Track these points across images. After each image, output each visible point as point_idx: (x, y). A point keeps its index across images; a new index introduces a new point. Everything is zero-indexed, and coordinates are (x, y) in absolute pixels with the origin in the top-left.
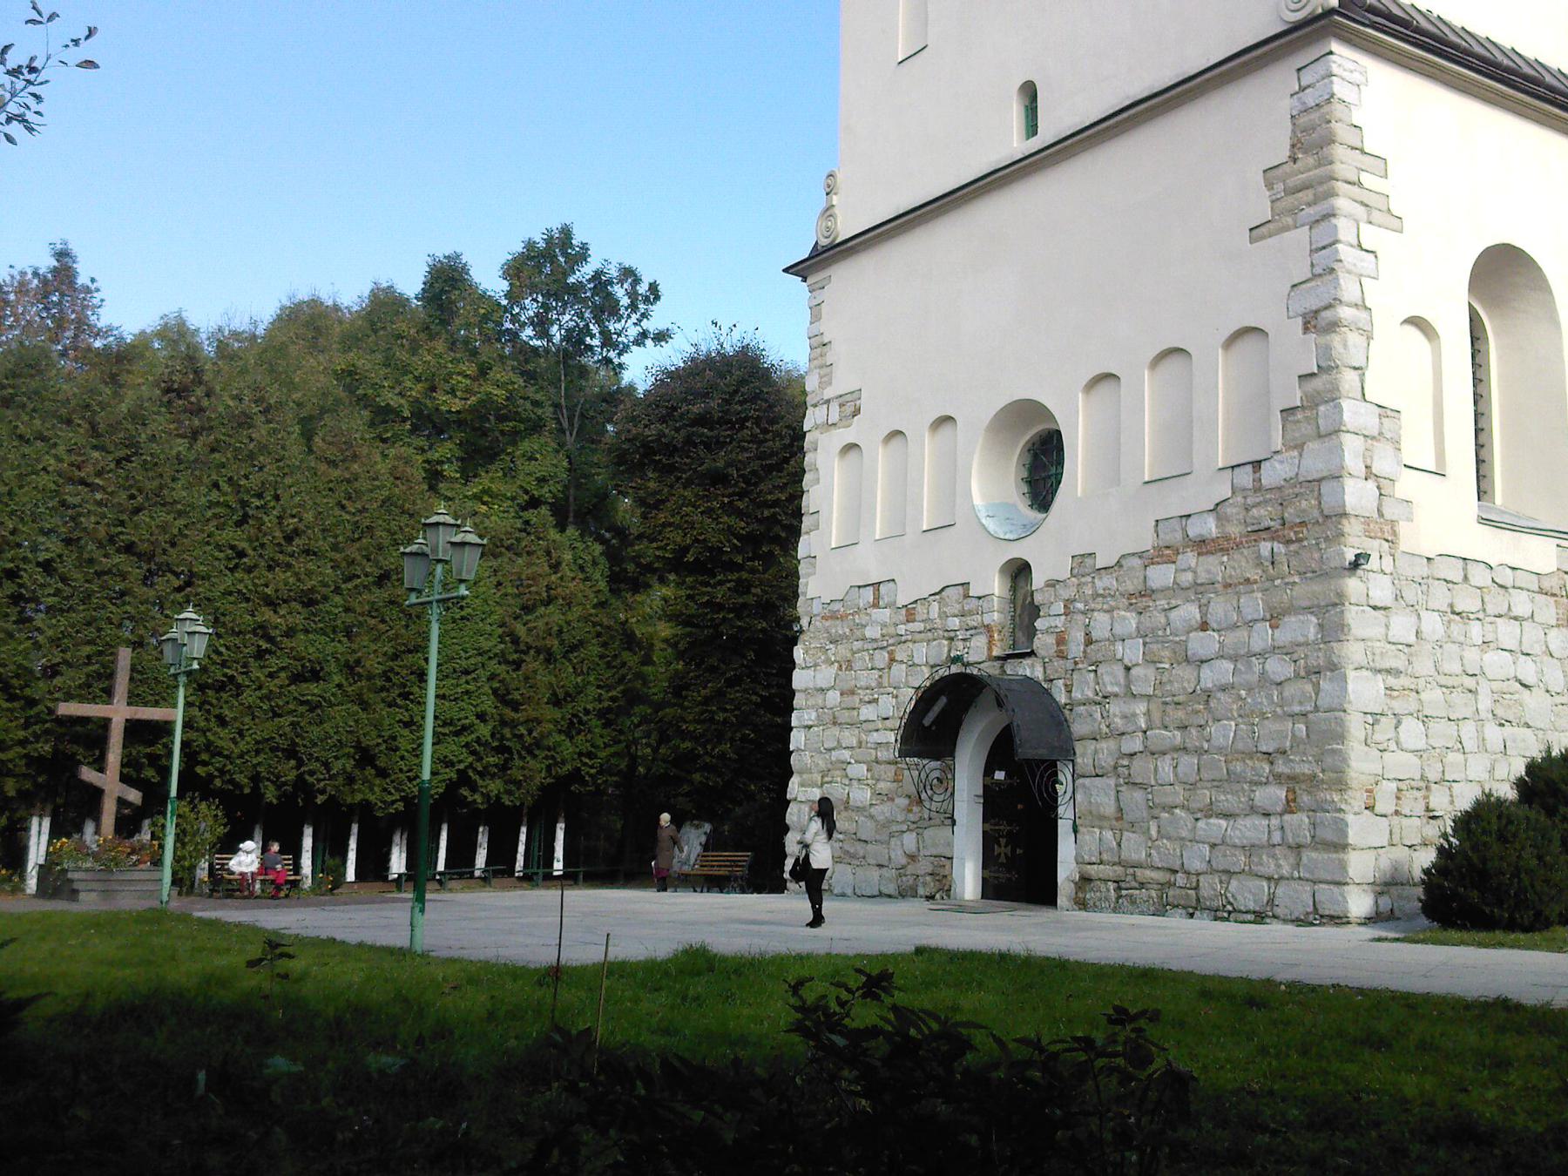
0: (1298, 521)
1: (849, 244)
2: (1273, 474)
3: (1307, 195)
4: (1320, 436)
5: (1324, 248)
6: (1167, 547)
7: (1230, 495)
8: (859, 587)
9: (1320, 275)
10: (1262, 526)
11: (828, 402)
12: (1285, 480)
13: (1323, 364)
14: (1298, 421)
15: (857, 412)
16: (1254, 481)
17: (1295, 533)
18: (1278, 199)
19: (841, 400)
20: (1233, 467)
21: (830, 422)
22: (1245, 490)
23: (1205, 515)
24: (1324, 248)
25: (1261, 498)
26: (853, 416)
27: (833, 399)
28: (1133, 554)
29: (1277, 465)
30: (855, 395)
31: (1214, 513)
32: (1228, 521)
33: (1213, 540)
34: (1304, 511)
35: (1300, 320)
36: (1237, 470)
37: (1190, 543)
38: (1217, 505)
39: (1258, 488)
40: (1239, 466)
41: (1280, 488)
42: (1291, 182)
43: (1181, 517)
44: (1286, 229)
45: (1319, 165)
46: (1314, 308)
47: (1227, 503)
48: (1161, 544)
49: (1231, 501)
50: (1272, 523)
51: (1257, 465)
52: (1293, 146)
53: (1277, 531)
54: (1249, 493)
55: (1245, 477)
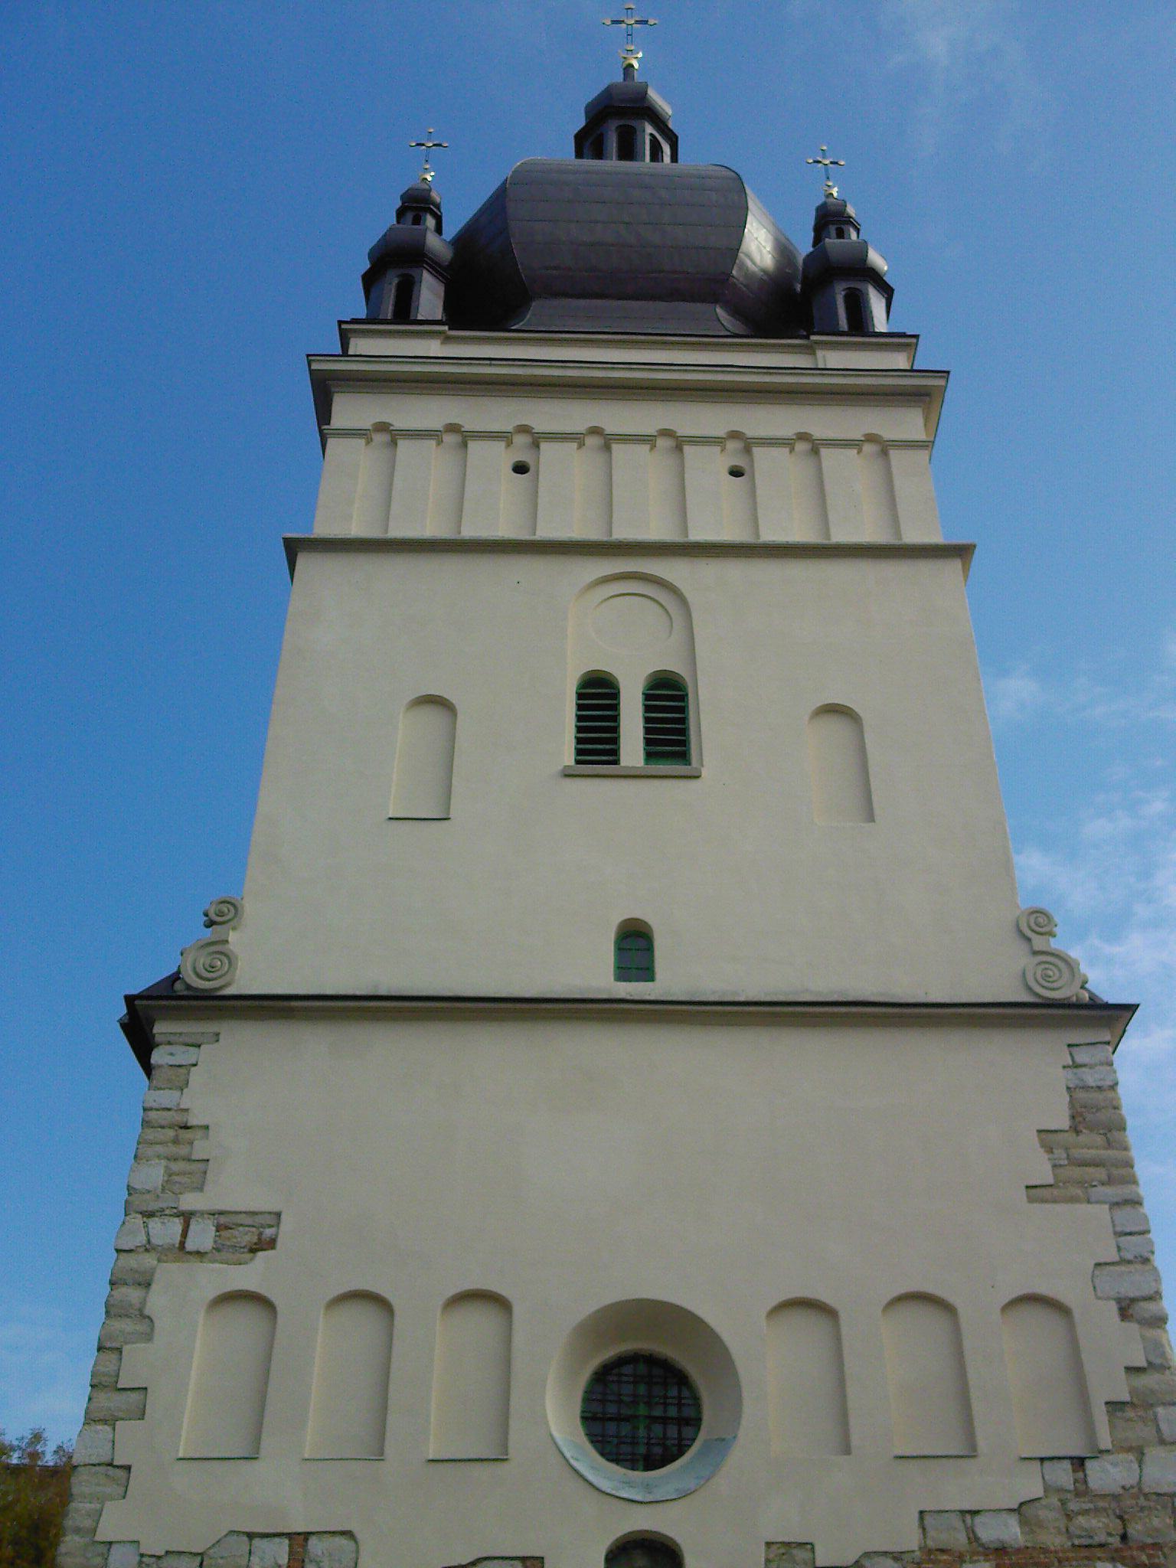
0: (1149, 1541)
1: (294, 1004)
2: (1107, 1475)
3: (1100, 1173)
4: (1162, 1442)
5: (1130, 1234)
6: (942, 1551)
7: (1040, 1493)
8: (251, 1536)
9: (1129, 1262)
10: (1097, 1540)
11: (187, 1217)
12: (1123, 1487)
13: (1152, 1358)
14: (1128, 1420)
15: (271, 1244)
16: (1076, 1481)
17: (1149, 1556)
18: (1061, 1166)
19: (223, 1220)
20: (1042, 1460)
21: (190, 1245)
22: (1061, 1490)
23: (1004, 1515)
24: (1130, 1234)
25: (1091, 1506)
26: (253, 1251)
27: (202, 1213)
28: (885, 1553)
29: (1109, 1467)
30: (269, 1220)
31: (1017, 1512)
32: (1041, 1527)
33: (1018, 1550)
34: (1157, 1530)
35: (1113, 1307)
36: (1047, 1464)
37: (980, 1549)
38: (1021, 1504)
39: (1082, 1490)
40: (1052, 1459)
41: (1115, 1497)
42: (1077, 1153)
43: (963, 1512)
44: (1073, 1200)
45: (1109, 1145)
46: (1132, 1295)
47: (1037, 1504)
48: (931, 1544)
49: (1043, 1502)
50: (1110, 1540)
51: (1079, 1463)
52: (1073, 1117)
53: (1117, 1550)
54: (1069, 1496)
55: (1063, 1476)
